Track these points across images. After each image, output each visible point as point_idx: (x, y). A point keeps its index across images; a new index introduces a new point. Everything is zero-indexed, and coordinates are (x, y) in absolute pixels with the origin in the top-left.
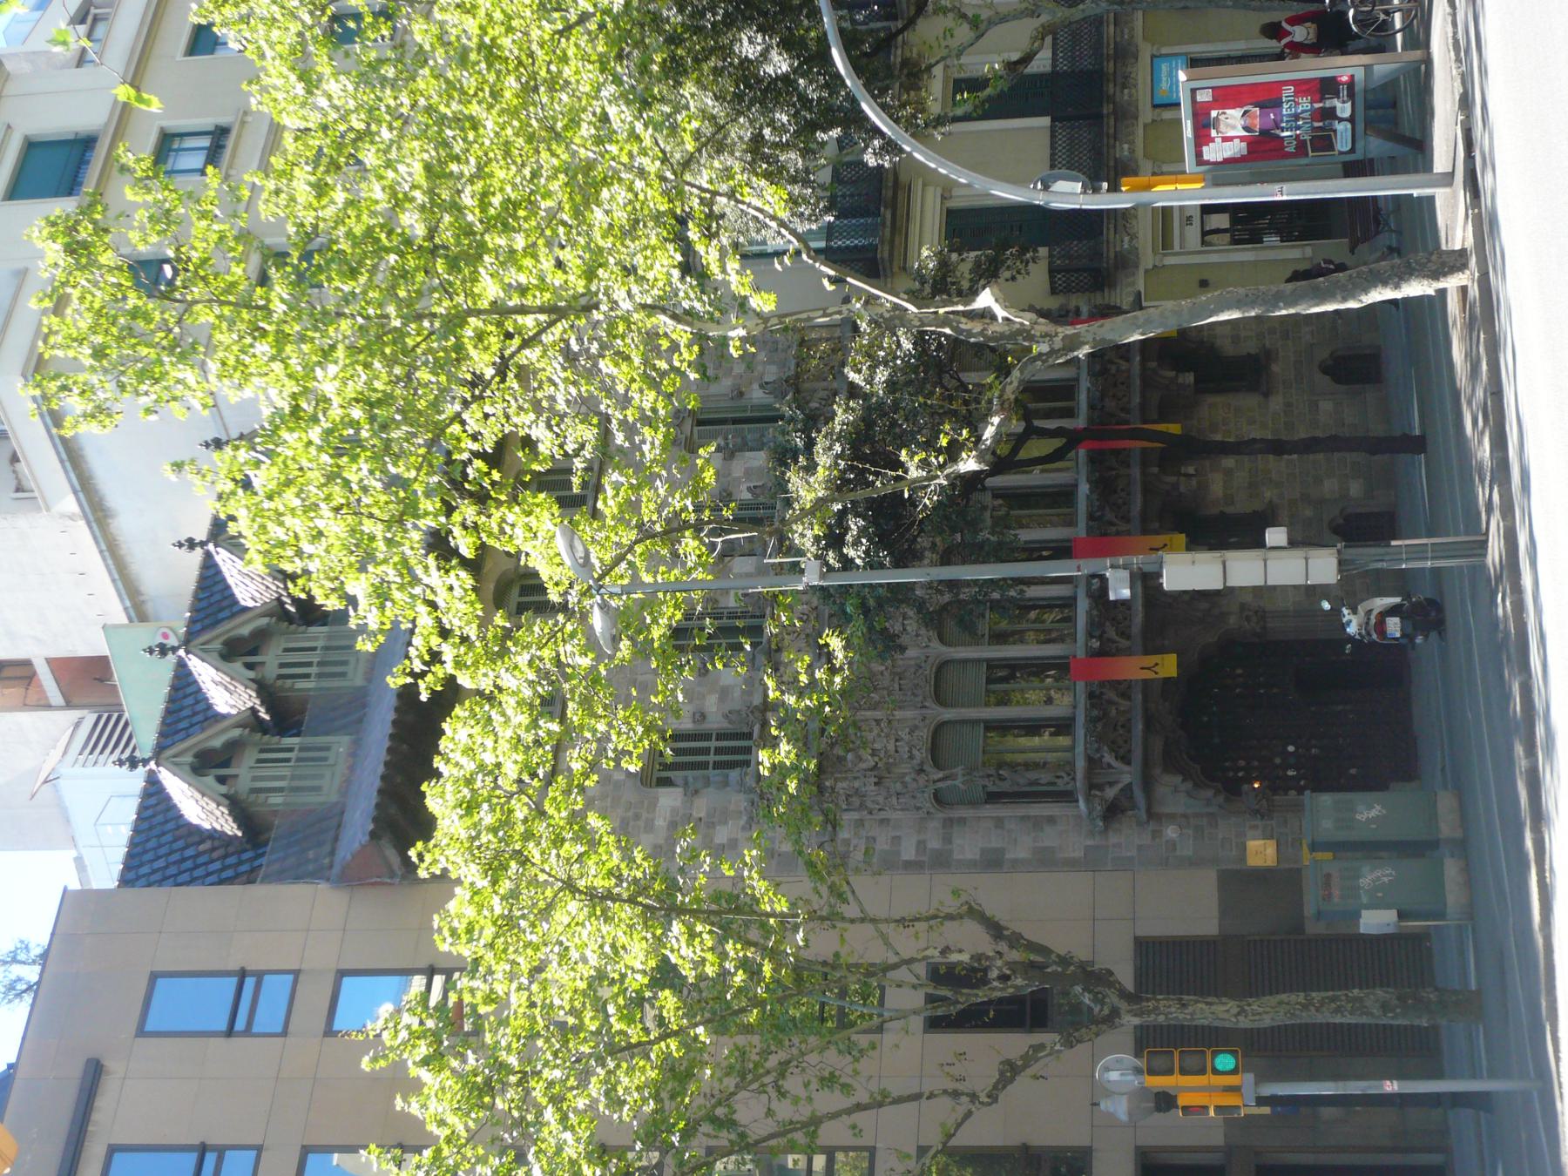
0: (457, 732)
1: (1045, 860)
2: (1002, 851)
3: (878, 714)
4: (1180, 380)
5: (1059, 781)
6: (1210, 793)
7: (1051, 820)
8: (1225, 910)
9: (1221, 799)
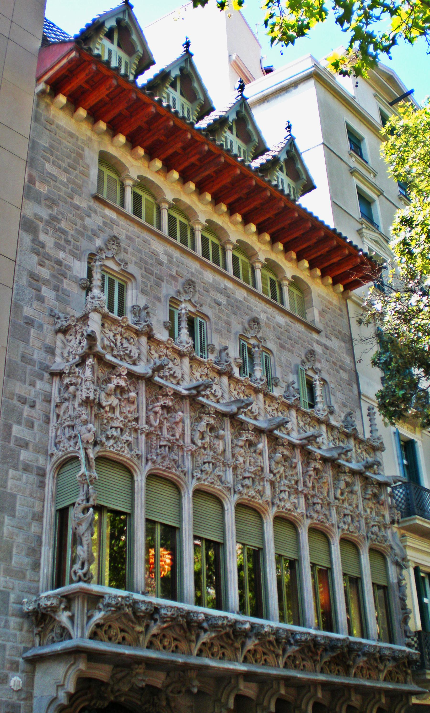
0: (72, 513)
3: (143, 420)
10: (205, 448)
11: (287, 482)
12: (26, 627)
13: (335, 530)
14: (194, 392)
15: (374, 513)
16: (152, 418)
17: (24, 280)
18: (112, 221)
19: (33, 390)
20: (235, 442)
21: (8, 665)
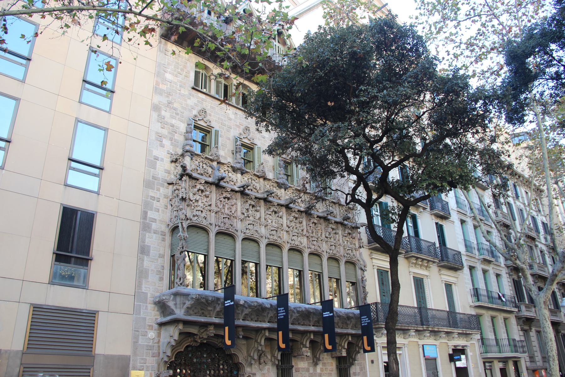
1: (141, 274)
2: (148, 255)
4: (343, 350)
5: (178, 280)
6: (169, 354)
7: (161, 279)
8: (109, 358)
9: (166, 359)
10: (249, 217)
11: (296, 231)
12: (156, 309)
13: (325, 253)
14: (242, 189)
15: (349, 243)
16: (218, 204)
17: (153, 137)
18: (203, 100)
19: (158, 192)
20: (267, 212)
21: (148, 328)
